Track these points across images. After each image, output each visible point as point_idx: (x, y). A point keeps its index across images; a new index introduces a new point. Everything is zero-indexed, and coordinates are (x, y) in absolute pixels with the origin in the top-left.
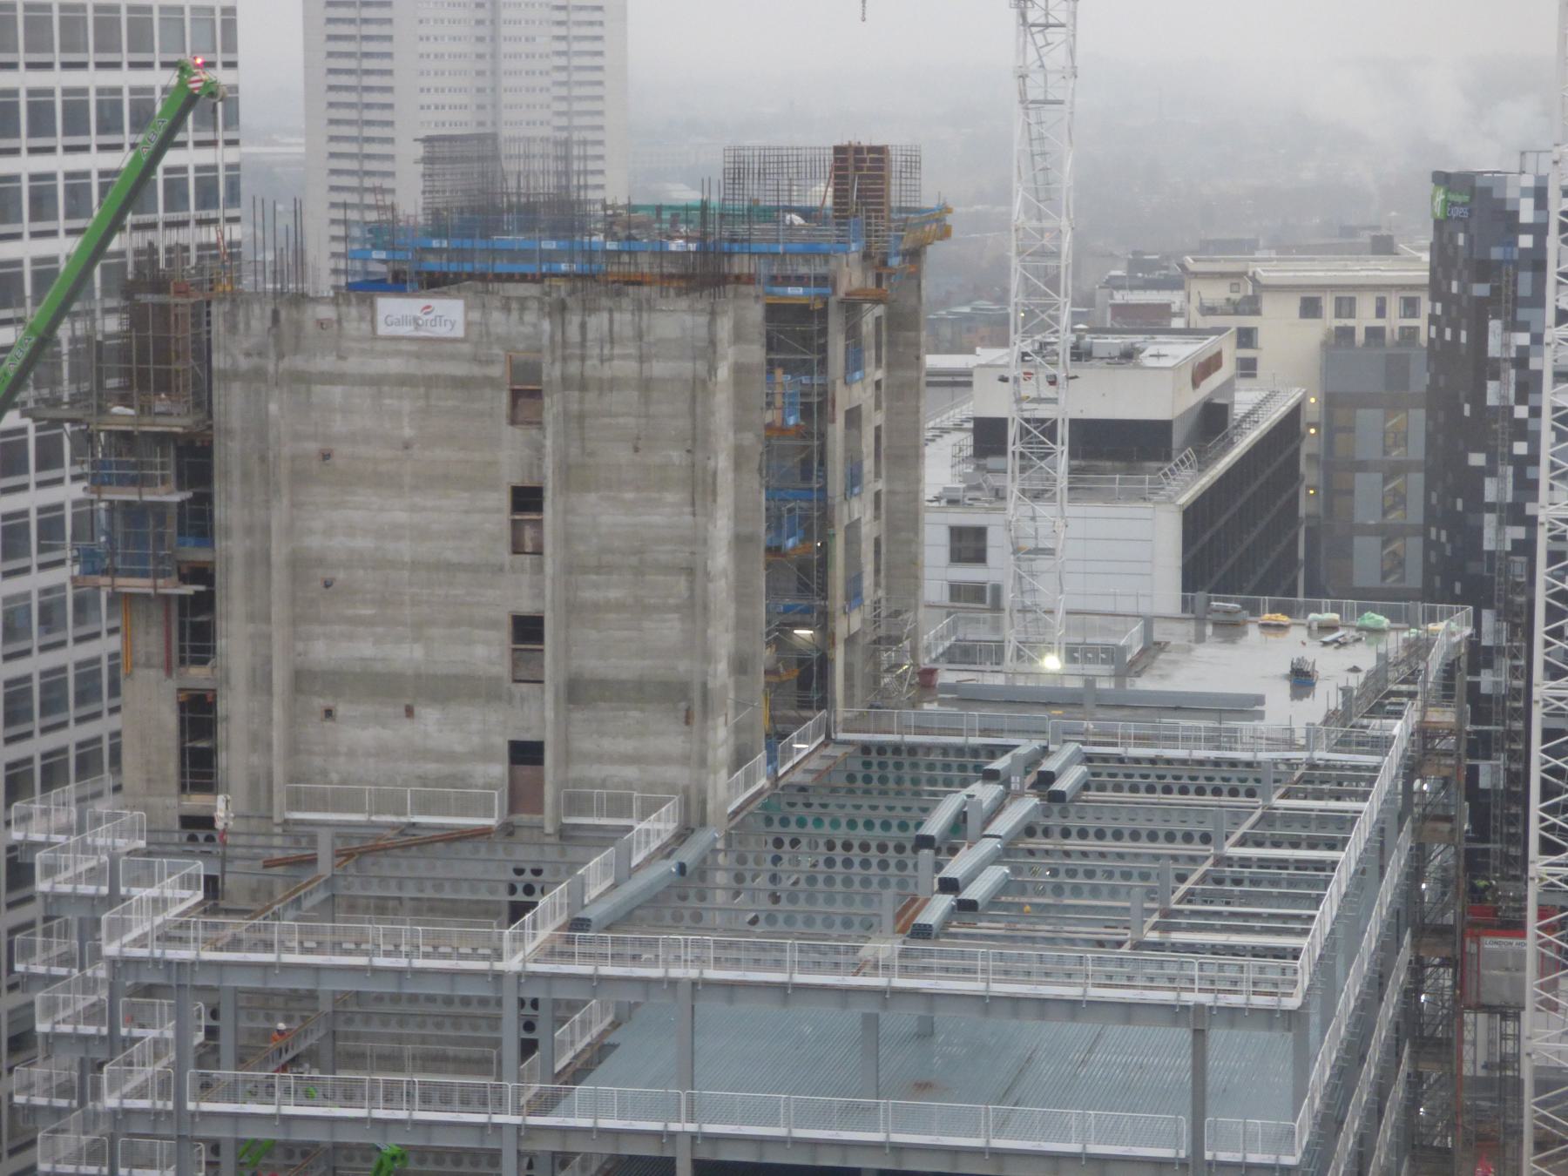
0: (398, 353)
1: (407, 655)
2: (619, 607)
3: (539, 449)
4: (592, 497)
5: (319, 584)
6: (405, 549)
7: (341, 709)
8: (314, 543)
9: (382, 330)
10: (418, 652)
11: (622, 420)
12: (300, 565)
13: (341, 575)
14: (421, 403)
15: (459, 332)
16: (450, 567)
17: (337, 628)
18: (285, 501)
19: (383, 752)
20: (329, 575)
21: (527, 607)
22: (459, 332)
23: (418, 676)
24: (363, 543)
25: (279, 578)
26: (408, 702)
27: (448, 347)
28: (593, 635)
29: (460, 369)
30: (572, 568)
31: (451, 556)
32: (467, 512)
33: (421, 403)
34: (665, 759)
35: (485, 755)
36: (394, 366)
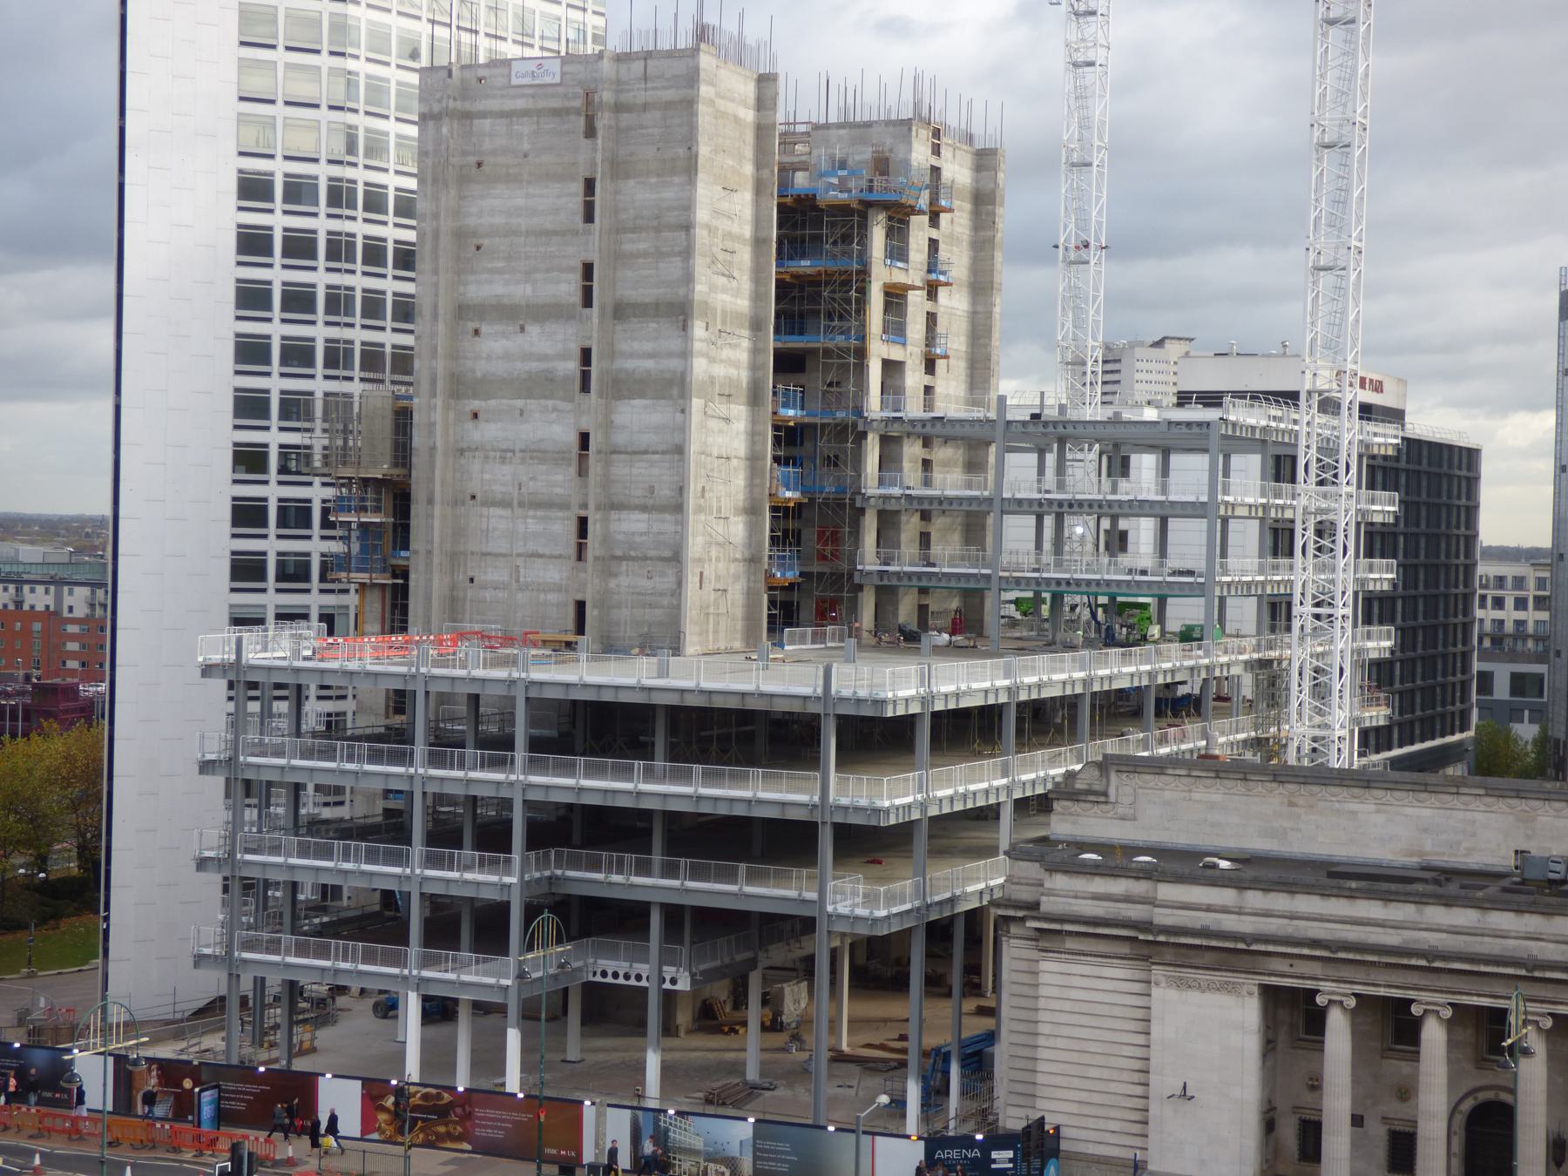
0: (523, 96)
1: (521, 292)
2: (645, 254)
3: (595, 150)
4: (631, 183)
5: (474, 248)
6: (522, 222)
7: (484, 329)
8: (471, 221)
9: (515, 81)
10: (529, 290)
11: (650, 131)
12: (460, 235)
13: (485, 242)
14: (535, 127)
15: (557, 80)
16: (548, 233)
17: (484, 276)
18: (453, 192)
19: (507, 356)
20: (479, 242)
21: (589, 260)
22: (557, 80)
23: (528, 306)
24: (499, 220)
25: (446, 241)
26: (522, 322)
27: (551, 90)
28: (629, 274)
29: (555, 103)
30: (619, 230)
31: (549, 226)
32: (558, 197)
33: (535, 127)
34: (670, 355)
35: (563, 356)
36: (520, 104)
